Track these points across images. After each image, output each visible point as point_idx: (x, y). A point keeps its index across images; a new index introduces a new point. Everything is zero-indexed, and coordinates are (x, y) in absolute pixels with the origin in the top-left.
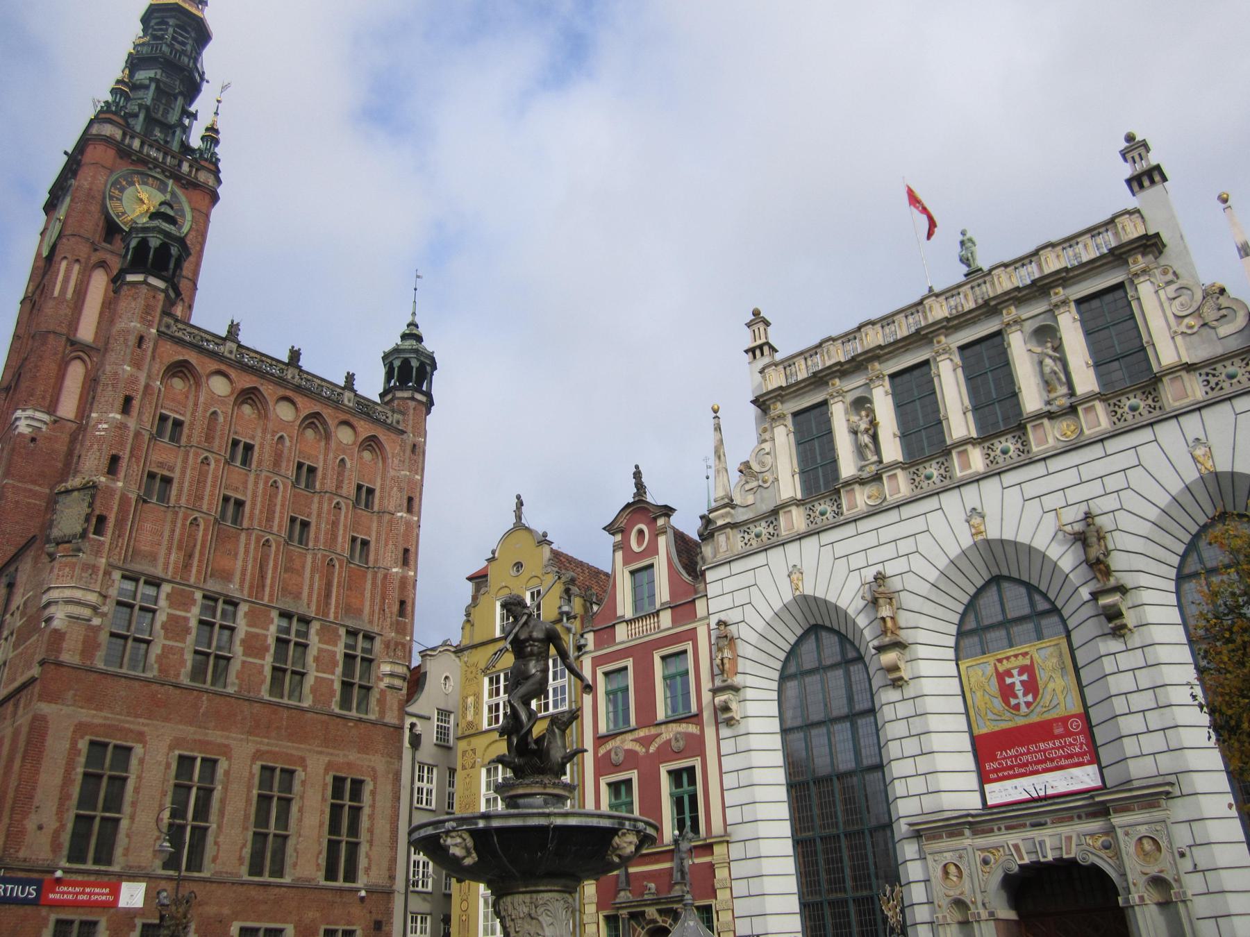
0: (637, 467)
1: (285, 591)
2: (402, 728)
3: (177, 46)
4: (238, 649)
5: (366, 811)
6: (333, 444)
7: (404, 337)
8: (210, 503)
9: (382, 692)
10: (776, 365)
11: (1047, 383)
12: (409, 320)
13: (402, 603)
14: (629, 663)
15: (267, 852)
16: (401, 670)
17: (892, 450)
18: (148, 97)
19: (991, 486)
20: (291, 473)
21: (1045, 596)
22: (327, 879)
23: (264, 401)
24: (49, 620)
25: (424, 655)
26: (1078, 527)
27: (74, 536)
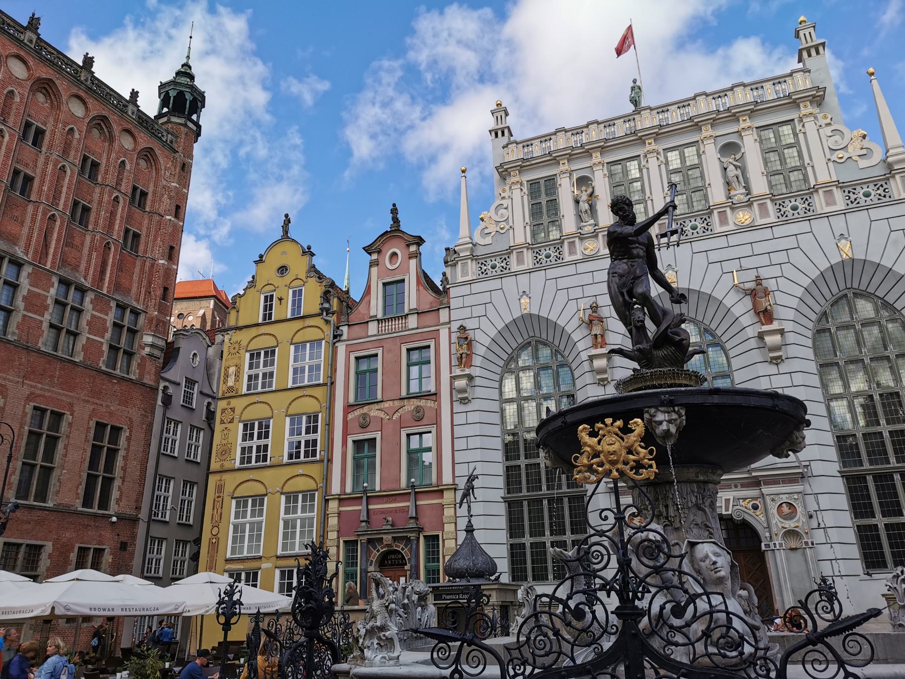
0: (394, 205)
4: (20, 303)
5: (122, 453)
7: (178, 73)
10: (517, 143)
11: (728, 184)
12: (185, 61)
16: (161, 343)
21: (713, 335)
23: (57, 95)
26: (752, 285)
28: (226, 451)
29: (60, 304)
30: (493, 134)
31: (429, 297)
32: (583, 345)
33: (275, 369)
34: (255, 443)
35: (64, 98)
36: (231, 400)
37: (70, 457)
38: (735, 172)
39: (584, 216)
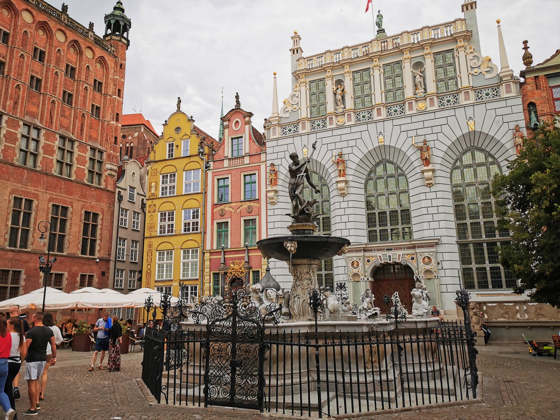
0: (237, 93)
1: (61, 126)
2: (115, 193)
4: (41, 151)
5: (99, 227)
10: (304, 59)
15: (57, 241)
19: (389, 124)
20: (64, 69)
21: (402, 170)
22: (82, 254)
26: (421, 145)
28: (152, 227)
29: (61, 149)
30: (292, 51)
31: (256, 146)
32: (333, 176)
33: (175, 184)
34: (167, 223)
36: (154, 200)
37: (73, 230)
38: (420, 79)
39: (339, 103)
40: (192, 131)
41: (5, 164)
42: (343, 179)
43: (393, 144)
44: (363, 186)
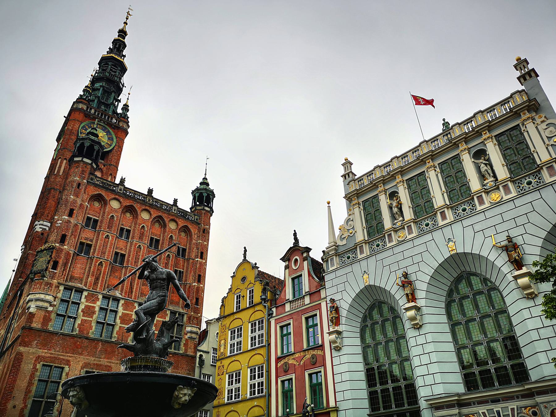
0: (295, 231)
2: (196, 357)
3: (113, 73)
4: (118, 321)
6: (167, 230)
7: (201, 184)
8: (109, 256)
9: (186, 340)
13: (197, 299)
14: (291, 321)
16: (194, 330)
17: (408, 214)
18: (99, 94)
19: (457, 227)
20: (147, 241)
21: (491, 282)
24: (29, 308)
25: (208, 323)
26: (503, 244)
27: (42, 270)
35: (139, 212)
38: (486, 168)
40: (256, 278)
41: (80, 338)
42: (413, 304)
43: (468, 250)
44: (443, 311)
